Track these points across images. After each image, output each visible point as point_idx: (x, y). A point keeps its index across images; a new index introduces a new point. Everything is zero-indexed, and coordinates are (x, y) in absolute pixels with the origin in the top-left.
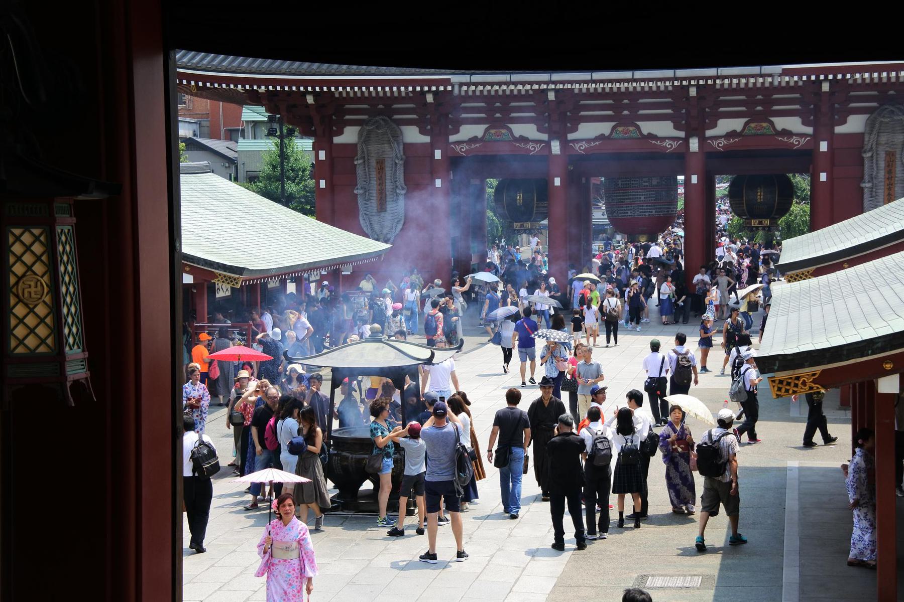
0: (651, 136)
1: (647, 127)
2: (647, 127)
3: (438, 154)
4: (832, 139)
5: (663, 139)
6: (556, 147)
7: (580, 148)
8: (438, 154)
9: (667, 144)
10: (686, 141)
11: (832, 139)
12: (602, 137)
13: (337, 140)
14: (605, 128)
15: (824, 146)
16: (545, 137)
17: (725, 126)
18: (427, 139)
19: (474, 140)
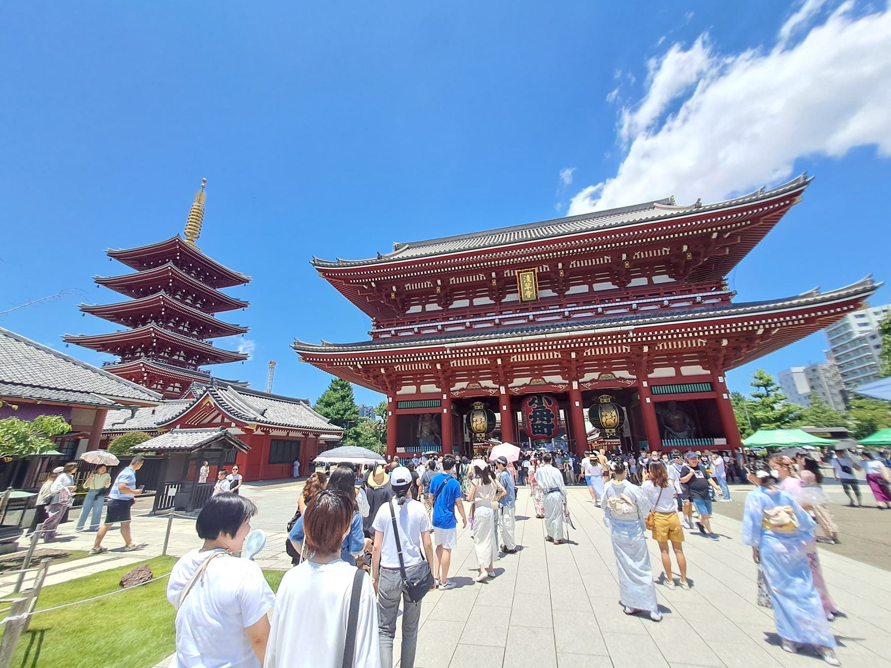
0: (551, 383)
1: (548, 379)
2: (548, 379)
3: (445, 397)
4: (648, 380)
5: (558, 384)
6: (503, 390)
7: (516, 391)
8: (445, 397)
9: (560, 386)
10: (570, 385)
11: (648, 380)
12: (525, 385)
13: (398, 393)
14: (527, 380)
15: (645, 384)
16: (497, 386)
17: (588, 377)
18: (440, 390)
19: (463, 389)
